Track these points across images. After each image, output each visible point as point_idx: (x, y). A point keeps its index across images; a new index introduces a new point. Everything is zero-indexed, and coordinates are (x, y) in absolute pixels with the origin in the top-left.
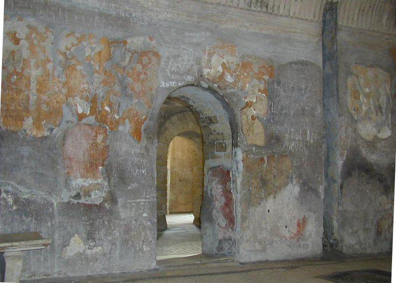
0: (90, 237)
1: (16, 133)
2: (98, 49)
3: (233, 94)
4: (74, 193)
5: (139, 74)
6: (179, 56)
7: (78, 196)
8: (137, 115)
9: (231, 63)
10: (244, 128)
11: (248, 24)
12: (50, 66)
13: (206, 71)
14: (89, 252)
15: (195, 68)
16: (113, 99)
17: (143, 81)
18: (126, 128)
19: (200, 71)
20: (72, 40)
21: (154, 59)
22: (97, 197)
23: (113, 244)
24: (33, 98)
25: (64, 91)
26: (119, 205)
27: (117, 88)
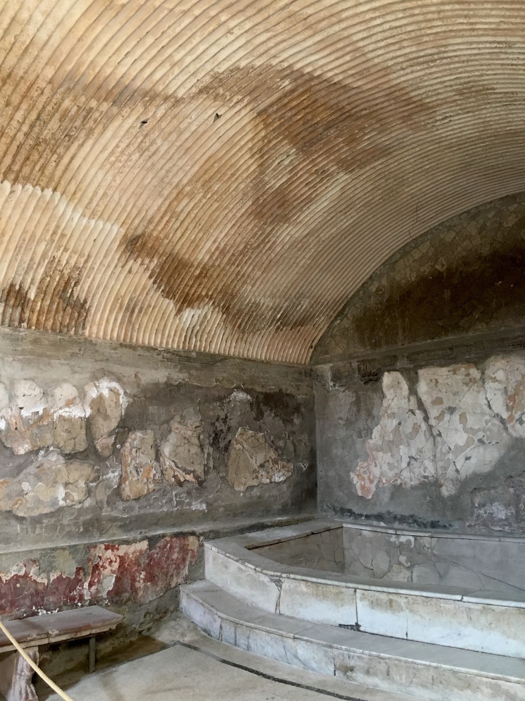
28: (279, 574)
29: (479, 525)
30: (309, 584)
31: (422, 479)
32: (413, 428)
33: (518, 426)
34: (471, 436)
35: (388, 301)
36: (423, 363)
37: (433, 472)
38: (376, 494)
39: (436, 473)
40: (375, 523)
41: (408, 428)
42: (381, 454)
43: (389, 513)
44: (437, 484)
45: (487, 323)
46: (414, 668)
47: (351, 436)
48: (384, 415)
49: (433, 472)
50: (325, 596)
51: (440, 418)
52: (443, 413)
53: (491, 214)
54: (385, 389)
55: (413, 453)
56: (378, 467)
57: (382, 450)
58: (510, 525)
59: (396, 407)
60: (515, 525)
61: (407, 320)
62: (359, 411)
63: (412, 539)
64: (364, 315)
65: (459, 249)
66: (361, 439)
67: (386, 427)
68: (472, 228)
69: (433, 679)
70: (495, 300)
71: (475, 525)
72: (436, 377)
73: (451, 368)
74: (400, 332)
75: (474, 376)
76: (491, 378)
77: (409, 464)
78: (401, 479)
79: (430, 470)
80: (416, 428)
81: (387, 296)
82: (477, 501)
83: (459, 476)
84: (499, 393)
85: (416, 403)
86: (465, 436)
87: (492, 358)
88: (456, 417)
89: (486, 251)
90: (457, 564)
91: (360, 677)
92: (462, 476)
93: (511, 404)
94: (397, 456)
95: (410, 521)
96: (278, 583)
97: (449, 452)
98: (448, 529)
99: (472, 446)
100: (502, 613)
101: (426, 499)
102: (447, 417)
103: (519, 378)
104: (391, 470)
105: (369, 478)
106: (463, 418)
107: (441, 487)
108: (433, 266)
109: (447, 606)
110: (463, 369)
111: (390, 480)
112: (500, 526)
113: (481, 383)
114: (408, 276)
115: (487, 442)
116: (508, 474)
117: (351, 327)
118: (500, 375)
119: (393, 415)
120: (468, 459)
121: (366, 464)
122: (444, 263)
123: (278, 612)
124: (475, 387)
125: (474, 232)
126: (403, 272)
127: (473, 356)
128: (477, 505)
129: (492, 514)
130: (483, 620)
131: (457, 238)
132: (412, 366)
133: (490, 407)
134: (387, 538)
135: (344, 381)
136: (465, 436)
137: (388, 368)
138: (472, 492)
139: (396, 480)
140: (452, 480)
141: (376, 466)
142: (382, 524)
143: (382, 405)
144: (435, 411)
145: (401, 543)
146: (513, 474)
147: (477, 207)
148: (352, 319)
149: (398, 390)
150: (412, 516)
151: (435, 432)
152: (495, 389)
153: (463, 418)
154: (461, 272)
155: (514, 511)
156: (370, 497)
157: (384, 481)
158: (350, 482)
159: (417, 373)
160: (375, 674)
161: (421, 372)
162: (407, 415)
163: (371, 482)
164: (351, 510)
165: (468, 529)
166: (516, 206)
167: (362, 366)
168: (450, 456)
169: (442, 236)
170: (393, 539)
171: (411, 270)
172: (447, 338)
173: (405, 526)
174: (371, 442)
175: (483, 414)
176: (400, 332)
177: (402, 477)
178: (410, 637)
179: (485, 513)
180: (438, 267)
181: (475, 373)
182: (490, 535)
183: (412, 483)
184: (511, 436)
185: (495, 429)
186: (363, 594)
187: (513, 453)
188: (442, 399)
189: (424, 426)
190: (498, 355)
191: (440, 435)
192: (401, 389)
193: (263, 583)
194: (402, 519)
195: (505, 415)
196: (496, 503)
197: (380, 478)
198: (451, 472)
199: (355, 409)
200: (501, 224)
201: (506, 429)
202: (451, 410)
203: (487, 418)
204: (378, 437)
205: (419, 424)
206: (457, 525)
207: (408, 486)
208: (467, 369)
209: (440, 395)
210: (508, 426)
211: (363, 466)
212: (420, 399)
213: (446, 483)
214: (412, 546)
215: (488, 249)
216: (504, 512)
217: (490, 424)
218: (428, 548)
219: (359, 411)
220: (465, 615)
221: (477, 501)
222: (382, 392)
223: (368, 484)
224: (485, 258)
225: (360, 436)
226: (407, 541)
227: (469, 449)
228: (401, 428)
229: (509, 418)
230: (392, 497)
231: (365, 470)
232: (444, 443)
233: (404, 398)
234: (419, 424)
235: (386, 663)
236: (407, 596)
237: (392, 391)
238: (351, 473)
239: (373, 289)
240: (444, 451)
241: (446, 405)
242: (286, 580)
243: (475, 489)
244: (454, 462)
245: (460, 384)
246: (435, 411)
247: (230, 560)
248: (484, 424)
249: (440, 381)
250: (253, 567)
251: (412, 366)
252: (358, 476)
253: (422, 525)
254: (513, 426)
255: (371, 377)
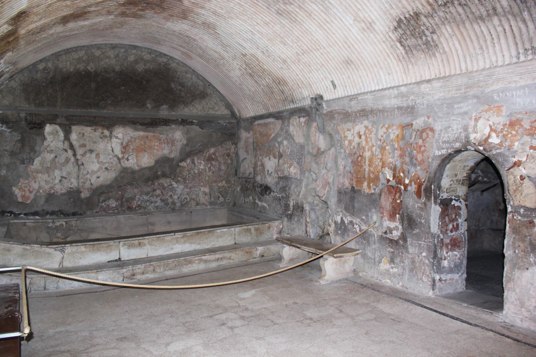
0: (392, 261)
1: (360, 190)
2: (397, 133)
3: (500, 154)
4: (384, 230)
5: (421, 147)
6: (449, 127)
7: (386, 233)
8: (419, 178)
9: (498, 124)
10: (510, 188)
11: (517, 78)
12: (374, 149)
13: (472, 137)
14: (391, 270)
15: (463, 135)
16: (405, 167)
17: (423, 152)
18: (413, 188)
19: (467, 137)
20: (384, 130)
21: (430, 133)
22: (396, 234)
23: (404, 269)
24: (367, 170)
25: (380, 164)
26: (409, 243)
27: (407, 159)
28: (63, 245)
29: (101, 211)
30: (87, 246)
31: (69, 189)
32: (66, 160)
33: (126, 161)
34: (101, 166)
35: (51, 78)
36: (75, 123)
37: (76, 185)
38: (34, 200)
39: (78, 185)
40: (32, 217)
41: (62, 159)
42: (40, 175)
43: (43, 210)
44: (79, 192)
45: (114, 107)
46: (167, 264)
47: (15, 163)
48: (44, 151)
49: (76, 185)
50: (98, 250)
51: (84, 155)
52: (85, 153)
53: (122, 50)
54: (46, 134)
55: (64, 174)
56: (37, 183)
57: (41, 172)
58: (117, 209)
59: (54, 146)
60: (120, 209)
61: (65, 94)
62: (23, 146)
63: (64, 223)
64: (31, 82)
65: (103, 62)
66: (25, 165)
67: (45, 158)
68: (111, 54)
69: (175, 265)
70: (120, 96)
71: (99, 212)
72: (83, 132)
73: (93, 128)
74: (59, 100)
75: (106, 134)
76: (115, 136)
77: (60, 181)
78: (54, 190)
79: (74, 183)
80: (67, 160)
81: (51, 75)
82: (102, 199)
83: (92, 187)
84: (119, 144)
85: (69, 145)
86: (98, 166)
87: (117, 126)
88: (94, 155)
89: (117, 68)
90: (93, 232)
91: (139, 277)
92: (95, 186)
93: (124, 150)
94: (52, 176)
95: (59, 213)
96: (62, 251)
97: (87, 174)
98: (83, 215)
99: (101, 171)
100: (190, 236)
101: (70, 200)
102: (88, 155)
103: (129, 138)
104: (46, 184)
105: (29, 190)
106: (98, 155)
107: (81, 192)
108: (86, 67)
109: (168, 239)
110: (100, 130)
111: (46, 191)
112: (112, 210)
113: (109, 138)
114: (68, 67)
115: (109, 169)
116: (119, 185)
117: (18, 88)
118: (120, 136)
119: (51, 151)
120: (98, 177)
121: (27, 181)
122: (93, 67)
123: (61, 266)
124: (106, 140)
125: (112, 56)
126: (64, 63)
127: (106, 123)
128: (101, 201)
129: (108, 205)
130: (182, 240)
131: (102, 56)
132: (68, 123)
133: (113, 151)
134: (46, 225)
135: (11, 125)
136: (98, 166)
137: (50, 121)
138: (99, 195)
139: (51, 191)
140: (88, 189)
141: (35, 182)
142: (37, 217)
143: (43, 144)
144: (81, 151)
145: (56, 227)
146: (121, 185)
147: (117, 44)
148: (19, 82)
149: (56, 136)
150: (60, 211)
151: (80, 163)
152: (117, 142)
153: (98, 155)
154: (103, 76)
155: (120, 203)
156: (29, 202)
157: (41, 191)
158: (12, 194)
159: (70, 128)
160: (147, 273)
161: (73, 128)
162: (62, 152)
163: (31, 192)
164: (12, 211)
165: (96, 214)
166: (135, 51)
167: (28, 118)
168: (88, 176)
169: (93, 51)
170: (50, 225)
171: (71, 64)
172: (91, 110)
173: (54, 217)
174: (32, 167)
175: (109, 154)
176: (59, 100)
177: (55, 189)
178: (149, 256)
179: (105, 205)
180: (89, 68)
181: (106, 132)
182: (108, 215)
183: (62, 192)
184: (122, 166)
185: (115, 163)
186: (124, 244)
187: (122, 175)
188: (86, 144)
189: (73, 159)
190: (120, 125)
191: (83, 164)
192: (59, 136)
193: (49, 253)
194: (53, 213)
195: (120, 156)
196: (112, 200)
197: (38, 190)
198: (87, 185)
199: (19, 145)
200: (127, 58)
201: (120, 163)
202: (91, 151)
203: (111, 157)
204: (38, 164)
205: (70, 158)
206: (88, 213)
207: (59, 193)
208: (102, 130)
209: (85, 142)
210: (121, 161)
211: (25, 182)
212: (72, 143)
213: (84, 191)
214: (65, 226)
215: (118, 68)
216: (115, 204)
217: (112, 160)
218: (75, 226)
219: (23, 146)
220: (175, 241)
221: (102, 199)
222: (44, 136)
223: (27, 194)
224: (117, 72)
225: (23, 162)
226: (60, 225)
227: (99, 173)
228: (57, 160)
229: (122, 157)
230: (47, 201)
231: (26, 185)
232: (85, 169)
233: (61, 141)
234: (70, 158)
235: (153, 266)
236: (148, 239)
237: (52, 136)
238: (13, 188)
239: (41, 67)
240: (84, 173)
241: (88, 148)
242: (69, 248)
243: (101, 193)
244: (90, 180)
245: (98, 137)
246: (81, 151)
247: (14, 245)
248: (109, 160)
249: (86, 134)
250: (39, 246)
251: (68, 123)
252: (19, 189)
253: (66, 215)
254: (124, 162)
255: (36, 126)
